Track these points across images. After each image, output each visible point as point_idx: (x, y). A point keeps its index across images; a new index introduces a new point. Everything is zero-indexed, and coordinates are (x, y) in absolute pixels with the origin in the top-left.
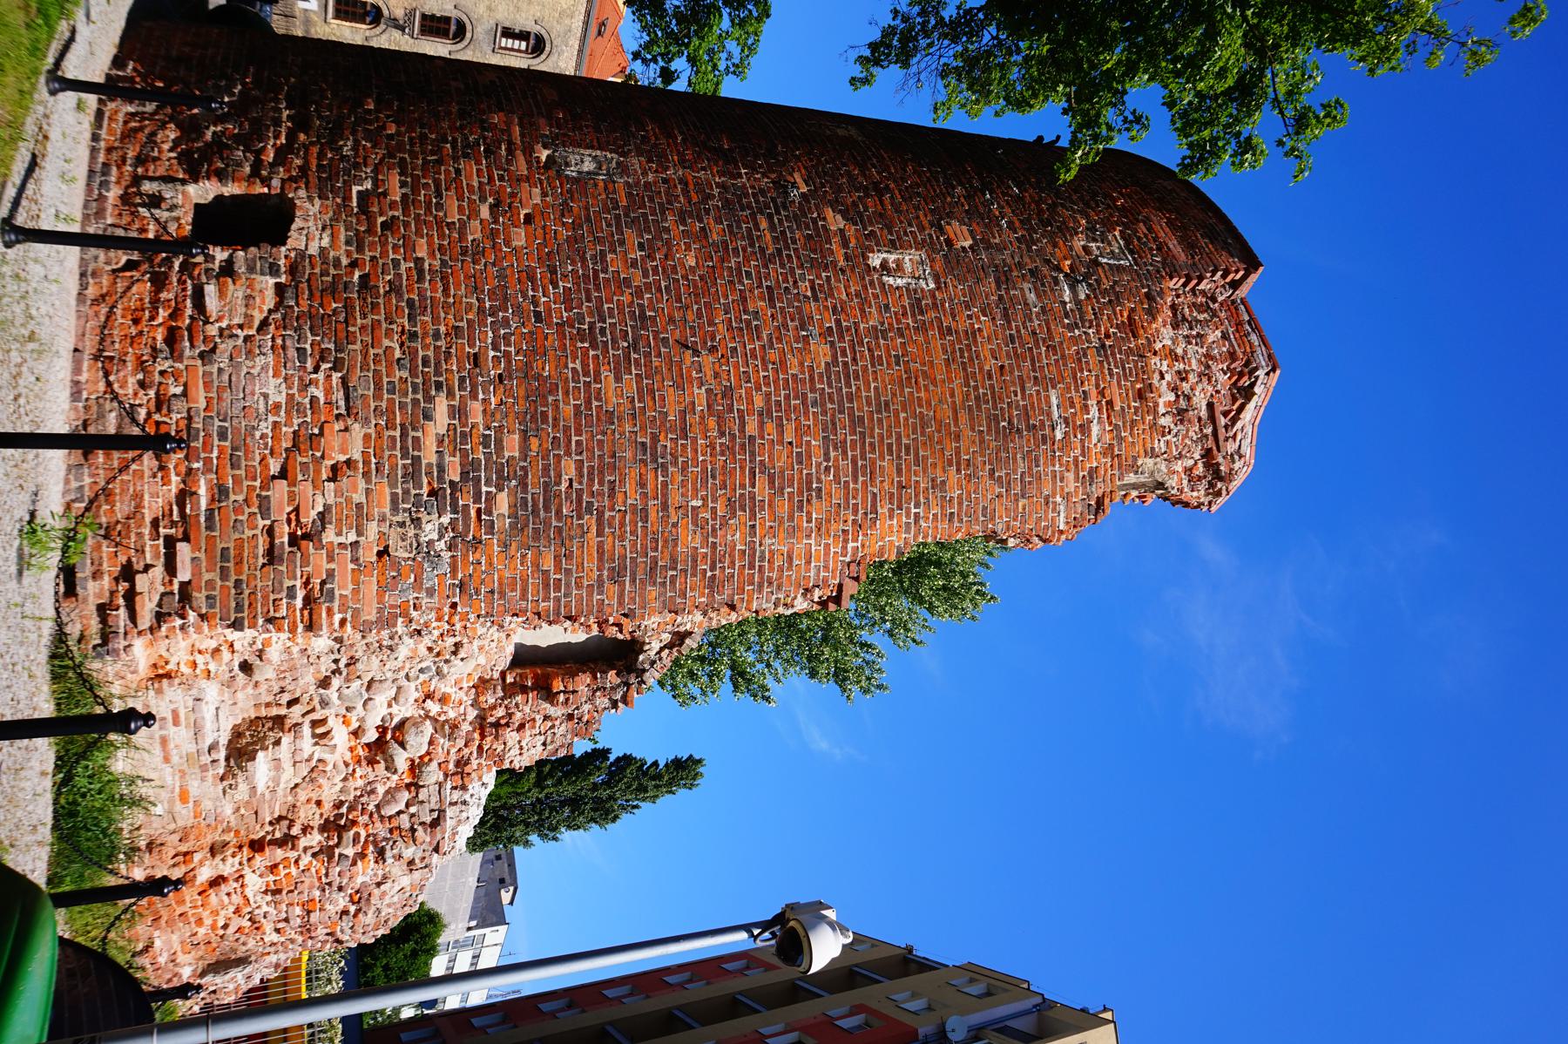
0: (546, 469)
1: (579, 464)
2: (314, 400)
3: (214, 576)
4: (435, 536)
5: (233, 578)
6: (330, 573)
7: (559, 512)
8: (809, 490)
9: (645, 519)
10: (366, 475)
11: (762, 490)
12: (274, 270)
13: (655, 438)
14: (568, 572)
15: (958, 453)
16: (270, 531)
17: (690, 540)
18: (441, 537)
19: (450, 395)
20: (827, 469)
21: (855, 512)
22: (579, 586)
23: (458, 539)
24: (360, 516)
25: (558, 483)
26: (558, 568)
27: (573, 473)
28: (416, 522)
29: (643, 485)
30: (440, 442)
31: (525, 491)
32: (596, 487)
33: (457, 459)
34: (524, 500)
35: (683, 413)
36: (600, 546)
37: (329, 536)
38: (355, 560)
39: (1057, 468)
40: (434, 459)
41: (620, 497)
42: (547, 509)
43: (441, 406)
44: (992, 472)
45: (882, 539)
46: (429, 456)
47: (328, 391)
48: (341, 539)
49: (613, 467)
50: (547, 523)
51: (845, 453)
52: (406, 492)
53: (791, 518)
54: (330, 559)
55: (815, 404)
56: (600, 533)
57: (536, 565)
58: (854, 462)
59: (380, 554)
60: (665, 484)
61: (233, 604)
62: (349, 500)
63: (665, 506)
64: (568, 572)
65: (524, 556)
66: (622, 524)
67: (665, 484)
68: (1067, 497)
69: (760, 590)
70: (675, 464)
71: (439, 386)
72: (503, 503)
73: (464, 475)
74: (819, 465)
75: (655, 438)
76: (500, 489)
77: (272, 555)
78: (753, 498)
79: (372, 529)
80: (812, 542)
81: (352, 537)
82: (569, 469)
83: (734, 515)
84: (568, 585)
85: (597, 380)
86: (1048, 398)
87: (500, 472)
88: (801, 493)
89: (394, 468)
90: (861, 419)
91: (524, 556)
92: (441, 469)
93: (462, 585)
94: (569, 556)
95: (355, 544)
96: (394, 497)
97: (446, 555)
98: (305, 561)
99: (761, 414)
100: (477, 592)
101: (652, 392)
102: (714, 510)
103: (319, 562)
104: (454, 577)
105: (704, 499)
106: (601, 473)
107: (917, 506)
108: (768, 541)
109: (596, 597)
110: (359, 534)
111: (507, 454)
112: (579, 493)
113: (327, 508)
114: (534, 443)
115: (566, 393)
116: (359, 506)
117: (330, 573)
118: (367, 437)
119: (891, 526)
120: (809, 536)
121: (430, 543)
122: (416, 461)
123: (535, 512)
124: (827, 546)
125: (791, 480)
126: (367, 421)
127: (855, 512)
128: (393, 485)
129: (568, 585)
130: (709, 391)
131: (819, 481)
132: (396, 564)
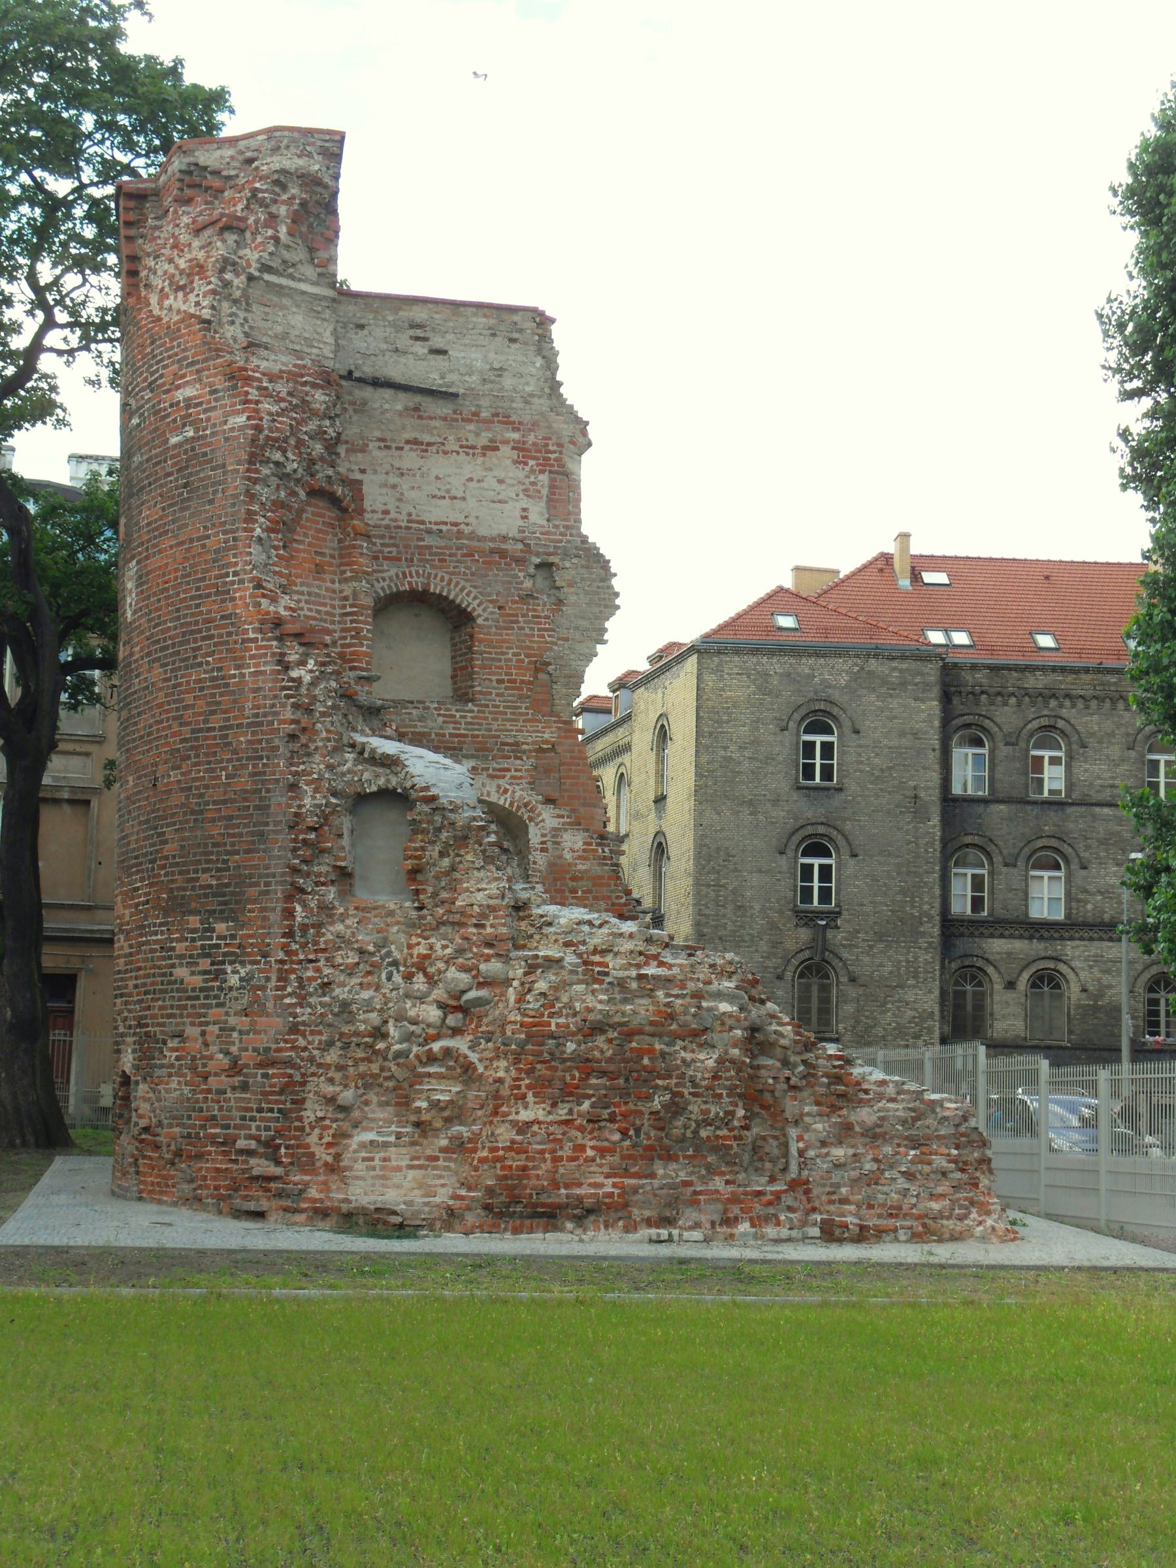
0: (206, 896)
1: (205, 871)
2: (178, 1059)
3: (253, 1124)
4: (237, 976)
5: (255, 1114)
6: (255, 1050)
7: (227, 885)
8: (220, 681)
9: (231, 818)
10: (207, 1024)
11: (216, 721)
12: (137, 1083)
13: (193, 812)
14: (260, 876)
15: (199, 539)
16: (234, 1088)
17: (244, 781)
18: (237, 972)
19: (173, 966)
20: (208, 663)
21: (229, 634)
22: (267, 867)
23: (236, 959)
24: (226, 1030)
25: (210, 886)
26: (257, 884)
27: (206, 875)
28: (231, 989)
29: (213, 820)
30: (193, 973)
31: (214, 911)
32: (214, 857)
33: (200, 961)
34: (222, 912)
35: (182, 790)
36: (247, 852)
37: (234, 1049)
38: (248, 1033)
39: (208, 432)
40: (200, 977)
41: (219, 839)
42: (224, 895)
43: (181, 972)
44: (211, 502)
45: (247, 605)
46: (198, 981)
47: (173, 1050)
48: (237, 1042)
49: (206, 845)
50: (233, 894)
51: (199, 648)
52: (216, 997)
53: (233, 693)
54: (246, 1050)
55: (176, 677)
56: (237, 853)
57: (254, 902)
58: (204, 639)
59: (246, 1015)
60: (215, 803)
61: (269, 1114)
62: (218, 1037)
63: (224, 802)
64: (260, 876)
65: (250, 911)
66: (233, 835)
67: (215, 803)
68: (227, 415)
69: (277, 714)
70: (201, 796)
71: (171, 975)
72: (221, 927)
73: (208, 955)
74: (206, 672)
75: (193, 812)
76: (213, 930)
77: (244, 1087)
78: (221, 728)
79: (232, 1021)
80: (246, 671)
81: (235, 1035)
82: (206, 879)
83: (230, 744)
84: (267, 876)
85: (167, 858)
86: (175, 446)
87: (206, 930)
88: (218, 687)
89: (204, 1006)
90: (184, 634)
91: (250, 911)
92: (205, 972)
93: (265, 956)
94: (251, 876)
95: (241, 1033)
96: (219, 1005)
97: (249, 967)
98: (247, 1066)
99: (181, 725)
100: (269, 945)
101: (173, 815)
102: (229, 761)
103: (247, 1058)
104: (258, 962)
105: (222, 769)
106: (206, 854)
107: (227, 575)
108: (247, 712)
109: (276, 852)
110: (233, 1029)
111: (198, 925)
112: (219, 870)
113: (221, 1051)
114: (193, 905)
115: (173, 881)
116: (221, 1029)
117: (255, 1050)
118: (193, 1024)
119: (241, 598)
120: (243, 675)
121: (241, 980)
122: (202, 990)
123: (225, 903)
124: (252, 657)
125: (213, 695)
126: (184, 1024)
127: (229, 634)
128: (209, 1006)
129: (267, 876)
130: (173, 768)
131: (212, 670)
132: (251, 1004)
